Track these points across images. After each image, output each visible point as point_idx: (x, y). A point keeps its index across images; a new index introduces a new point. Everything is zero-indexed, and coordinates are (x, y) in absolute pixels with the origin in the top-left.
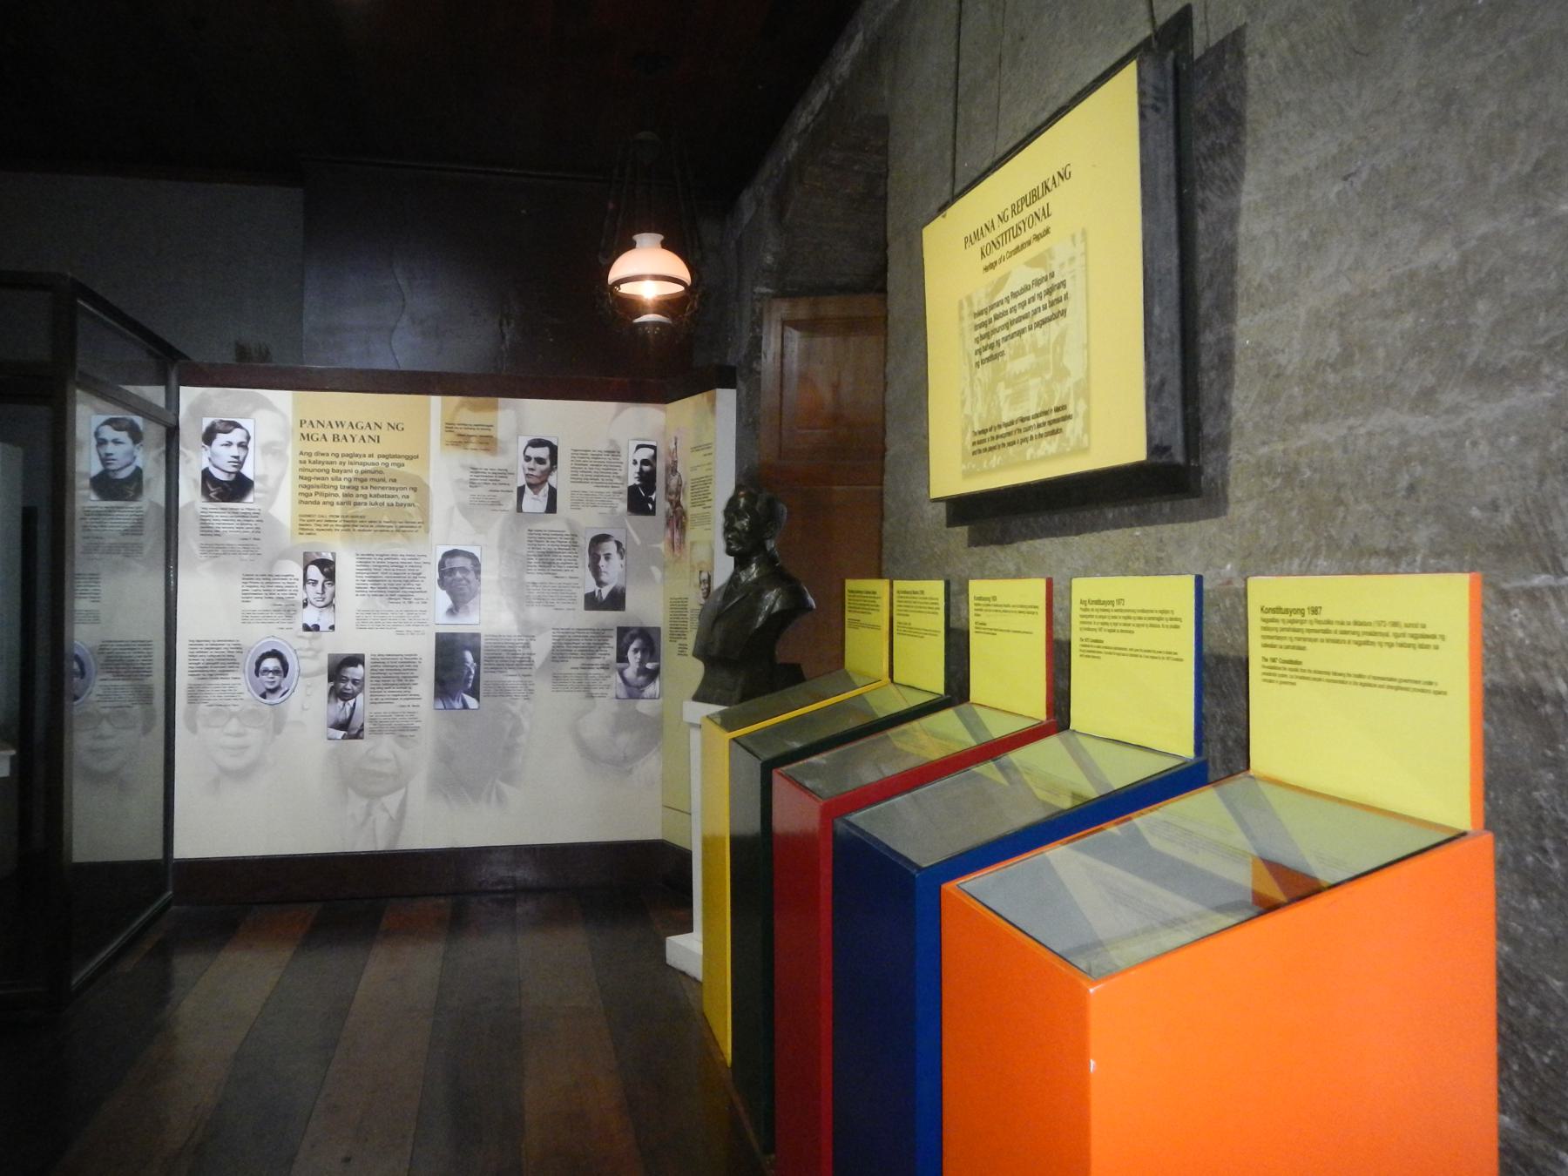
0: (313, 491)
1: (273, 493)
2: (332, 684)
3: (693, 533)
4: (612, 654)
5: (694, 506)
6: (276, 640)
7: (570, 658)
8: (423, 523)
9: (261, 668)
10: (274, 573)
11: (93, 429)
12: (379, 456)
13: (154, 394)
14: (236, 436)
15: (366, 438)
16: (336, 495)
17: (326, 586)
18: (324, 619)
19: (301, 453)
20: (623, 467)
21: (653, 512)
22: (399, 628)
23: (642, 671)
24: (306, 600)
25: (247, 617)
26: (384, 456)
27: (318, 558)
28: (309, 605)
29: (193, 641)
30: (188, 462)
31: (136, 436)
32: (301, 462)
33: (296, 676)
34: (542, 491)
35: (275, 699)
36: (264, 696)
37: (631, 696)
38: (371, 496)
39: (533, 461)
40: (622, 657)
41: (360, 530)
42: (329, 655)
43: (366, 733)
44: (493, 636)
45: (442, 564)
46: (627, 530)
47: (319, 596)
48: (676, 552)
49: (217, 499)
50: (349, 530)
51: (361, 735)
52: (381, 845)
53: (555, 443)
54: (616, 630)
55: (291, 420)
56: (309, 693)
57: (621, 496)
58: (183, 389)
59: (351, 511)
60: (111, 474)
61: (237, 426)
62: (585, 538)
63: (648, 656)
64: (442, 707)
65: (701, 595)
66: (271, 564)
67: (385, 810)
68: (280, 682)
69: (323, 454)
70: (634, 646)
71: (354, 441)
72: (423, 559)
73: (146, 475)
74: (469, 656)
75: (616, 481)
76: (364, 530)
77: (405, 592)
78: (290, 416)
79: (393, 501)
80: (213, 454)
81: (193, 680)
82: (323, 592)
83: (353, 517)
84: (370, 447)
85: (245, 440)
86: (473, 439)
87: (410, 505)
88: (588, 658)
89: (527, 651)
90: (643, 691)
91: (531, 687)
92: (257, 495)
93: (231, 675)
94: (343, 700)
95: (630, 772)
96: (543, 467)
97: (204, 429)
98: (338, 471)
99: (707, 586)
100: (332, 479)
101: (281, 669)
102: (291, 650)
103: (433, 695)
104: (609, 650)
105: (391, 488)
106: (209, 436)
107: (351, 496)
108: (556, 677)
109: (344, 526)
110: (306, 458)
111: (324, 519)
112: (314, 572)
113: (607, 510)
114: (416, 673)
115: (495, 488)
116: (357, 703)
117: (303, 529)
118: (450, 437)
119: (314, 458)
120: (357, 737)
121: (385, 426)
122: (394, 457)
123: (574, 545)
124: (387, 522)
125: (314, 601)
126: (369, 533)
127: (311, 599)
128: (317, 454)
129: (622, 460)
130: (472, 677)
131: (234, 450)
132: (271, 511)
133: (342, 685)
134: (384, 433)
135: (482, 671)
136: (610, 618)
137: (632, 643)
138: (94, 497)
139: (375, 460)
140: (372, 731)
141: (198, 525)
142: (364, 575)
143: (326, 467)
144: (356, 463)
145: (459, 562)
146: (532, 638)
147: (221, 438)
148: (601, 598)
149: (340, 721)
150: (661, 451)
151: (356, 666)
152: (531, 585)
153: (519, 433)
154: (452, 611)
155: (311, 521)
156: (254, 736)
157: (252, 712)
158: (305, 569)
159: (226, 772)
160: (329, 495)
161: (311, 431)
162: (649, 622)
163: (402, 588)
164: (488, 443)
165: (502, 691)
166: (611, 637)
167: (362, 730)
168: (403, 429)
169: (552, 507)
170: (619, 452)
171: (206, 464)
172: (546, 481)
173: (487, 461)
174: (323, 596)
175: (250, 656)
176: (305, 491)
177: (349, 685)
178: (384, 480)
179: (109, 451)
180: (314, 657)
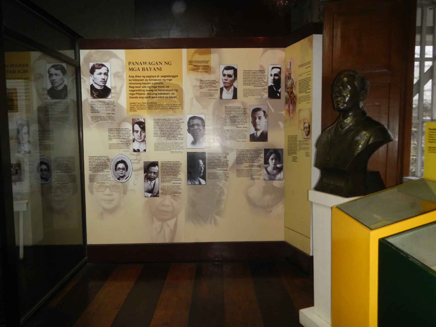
0: (135, 92)
1: (118, 94)
2: (146, 174)
3: (300, 106)
4: (262, 161)
5: (300, 92)
6: (123, 156)
7: (244, 162)
8: (180, 105)
9: (117, 168)
10: (121, 128)
11: (47, 70)
12: (162, 76)
13: (70, 53)
14: (103, 70)
15: (156, 69)
16: (144, 94)
17: (142, 133)
18: (142, 147)
19: (130, 76)
20: (266, 77)
21: (279, 98)
22: (172, 150)
23: (275, 168)
24: (134, 139)
25: (111, 147)
26: (163, 76)
27: (138, 121)
28: (135, 141)
29: (90, 157)
30: (85, 82)
31: (64, 72)
32: (129, 80)
33: (131, 171)
34: (231, 89)
35: (123, 180)
36: (119, 179)
37: (271, 179)
38: (159, 94)
39: (226, 76)
40: (266, 162)
41: (155, 109)
42: (144, 162)
43: (160, 195)
44: (211, 153)
45: (189, 123)
46: (268, 105)
47: (139, 137)
48: (291, 115)
49: (97, 97)
50: (150, 109)
51: (158, 195)
52: (167, 240)
53: (236, 68)
54: (263, 150)
55: (125, 63)
56: (137, 178)
57: (265, 91)
58: (81, 51)
59: (151, 100)
60: (55, 88)
61: (103, 65)
62: (250, 110)
63: (278, 162)
64: (191, 184)
65: (304, 134)
66: (119, 124)
67: (169, 226)
68: (125, 173)
69: (138, 77)
70: (271, 157)
71: (151, 70)
72: (181, 121)
73: (69, 88)
74: (201, 162)
75: (263, 84)
76: (156, 109)
77: (174, 135)
78: (124, 60)
79: (168, 96)
80: (94, 78)
81: (91, 173)
82: (141, 136)
83: (151, 103)
84: (158, 73)
85: (107, 72)
86: (201, 67)
87: (175, 97)
88: (251, 162)
89: (225, 159)
90: (276, 177)
91: (227, 175)
92: (113, 95)
93: (106, 170)
94: (150, 180)
95: (270, 212)
96: (231, 79)
97: (90, 68)
98: (145, 84)
99: (308, 130)
100: (143, 87)
101: (125, 168)
102: (129, 160)
103: (186, 179)
104: (261, 159)
105: (167, 90)
106: (92, 71)
107: (150, 94)
108: (238, 171)
109: (148, 107)
110: (132, 78)
111: (140, 104)
112: (137, 127)
113: (259, 97)
114: (179, 169)
115: (210, 88)
116: (156, 182)
117: (132, 109)
118: (191, 67)
119: (135, 78)
120: (156, 196)
121: (163, 63)
122: (168, 76)
123: (245, 113)
124: (166, 105)
125: (137, 139)
126: (159, 110)
127: (136, 138)
128: (136, 76)
129: (265, 74)
130: (202, 171)
131: (103, 76)
132: (118, 102)
133: (150, 174)
134: (163, 66)
135: (207, 168)
136: (261, 145)
137: (270, 156)
138: (49, 98)
139: (160, 78)
140: (162, 194)
141: (89, 108)
142: (157, 128)
143: (140, 82)
144: (152, 80)
145: (196, 121)
146: (228, 154)
147: (97, 71)
148: (257, 136)
149: (149, 189)
150: (283, 69)
151: (155, 166)
152: (227, 131)
153: (220, 64)
154: (194, 143)
155: (135, 105)
156: (116, 195)
157: (115, 186)
158: (133, 126)
159: (105, 210)
160: (141, 94)
161: (133, 66)
162: (278, 147)
163: (173, 133)
164: (207, 69)
165: (215, 177)
166: (262, 153)
167: (158, 193)
168: (171, 64)
169: (235, 97)
170: (264, 71)
171: (92, 82)
172: (232, 85)
173: (207, 77)
174: (141, 137)
175: (113, 162)
176: (132, 92)
177: (153, 175)
178: (164, 87)
179: (54, 79)
180: (138, 163)
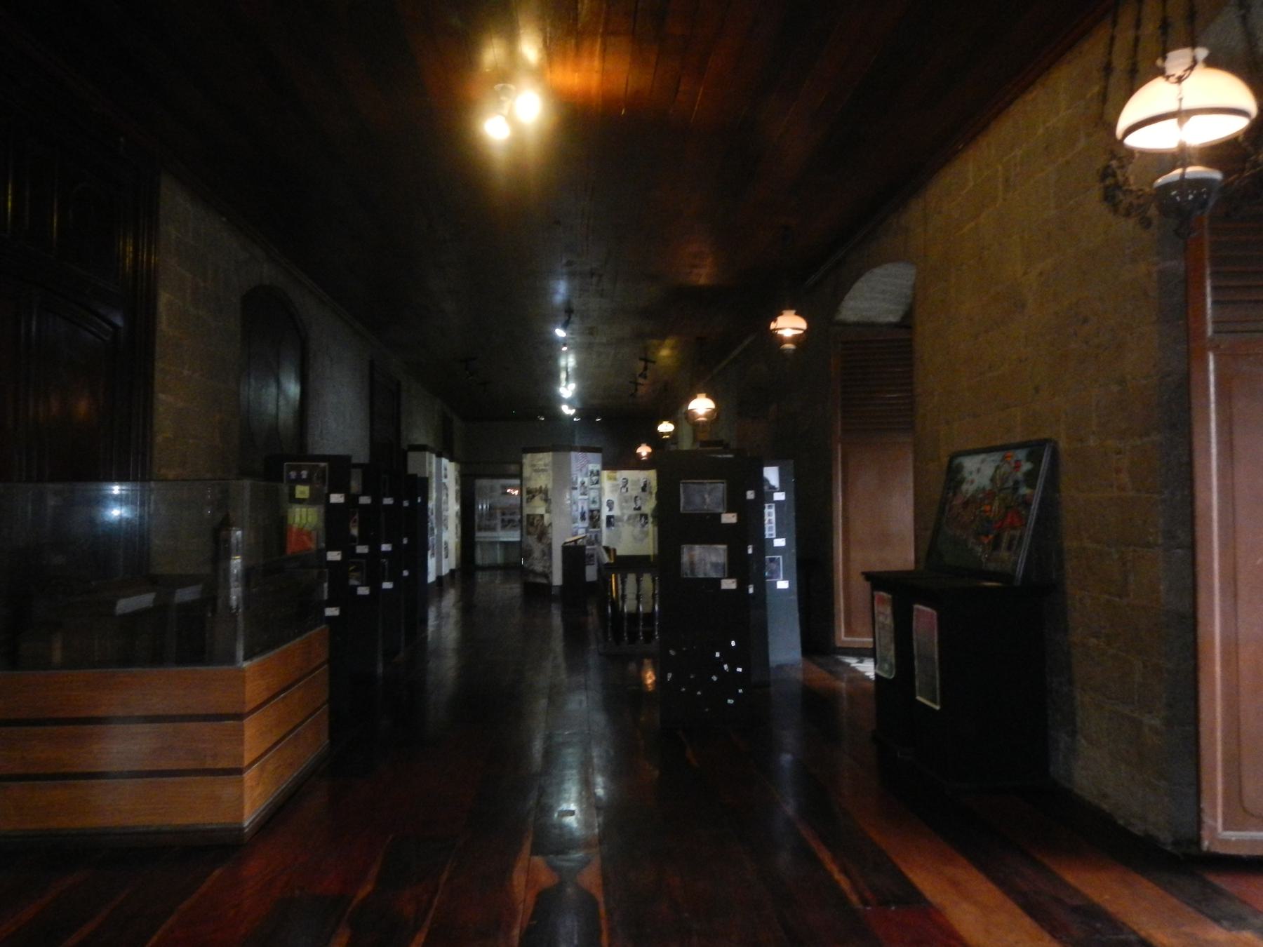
4: (639, 519)
40: (641, 519)
164: (615, 479)
165: (618, 526)
169: (627, 491)
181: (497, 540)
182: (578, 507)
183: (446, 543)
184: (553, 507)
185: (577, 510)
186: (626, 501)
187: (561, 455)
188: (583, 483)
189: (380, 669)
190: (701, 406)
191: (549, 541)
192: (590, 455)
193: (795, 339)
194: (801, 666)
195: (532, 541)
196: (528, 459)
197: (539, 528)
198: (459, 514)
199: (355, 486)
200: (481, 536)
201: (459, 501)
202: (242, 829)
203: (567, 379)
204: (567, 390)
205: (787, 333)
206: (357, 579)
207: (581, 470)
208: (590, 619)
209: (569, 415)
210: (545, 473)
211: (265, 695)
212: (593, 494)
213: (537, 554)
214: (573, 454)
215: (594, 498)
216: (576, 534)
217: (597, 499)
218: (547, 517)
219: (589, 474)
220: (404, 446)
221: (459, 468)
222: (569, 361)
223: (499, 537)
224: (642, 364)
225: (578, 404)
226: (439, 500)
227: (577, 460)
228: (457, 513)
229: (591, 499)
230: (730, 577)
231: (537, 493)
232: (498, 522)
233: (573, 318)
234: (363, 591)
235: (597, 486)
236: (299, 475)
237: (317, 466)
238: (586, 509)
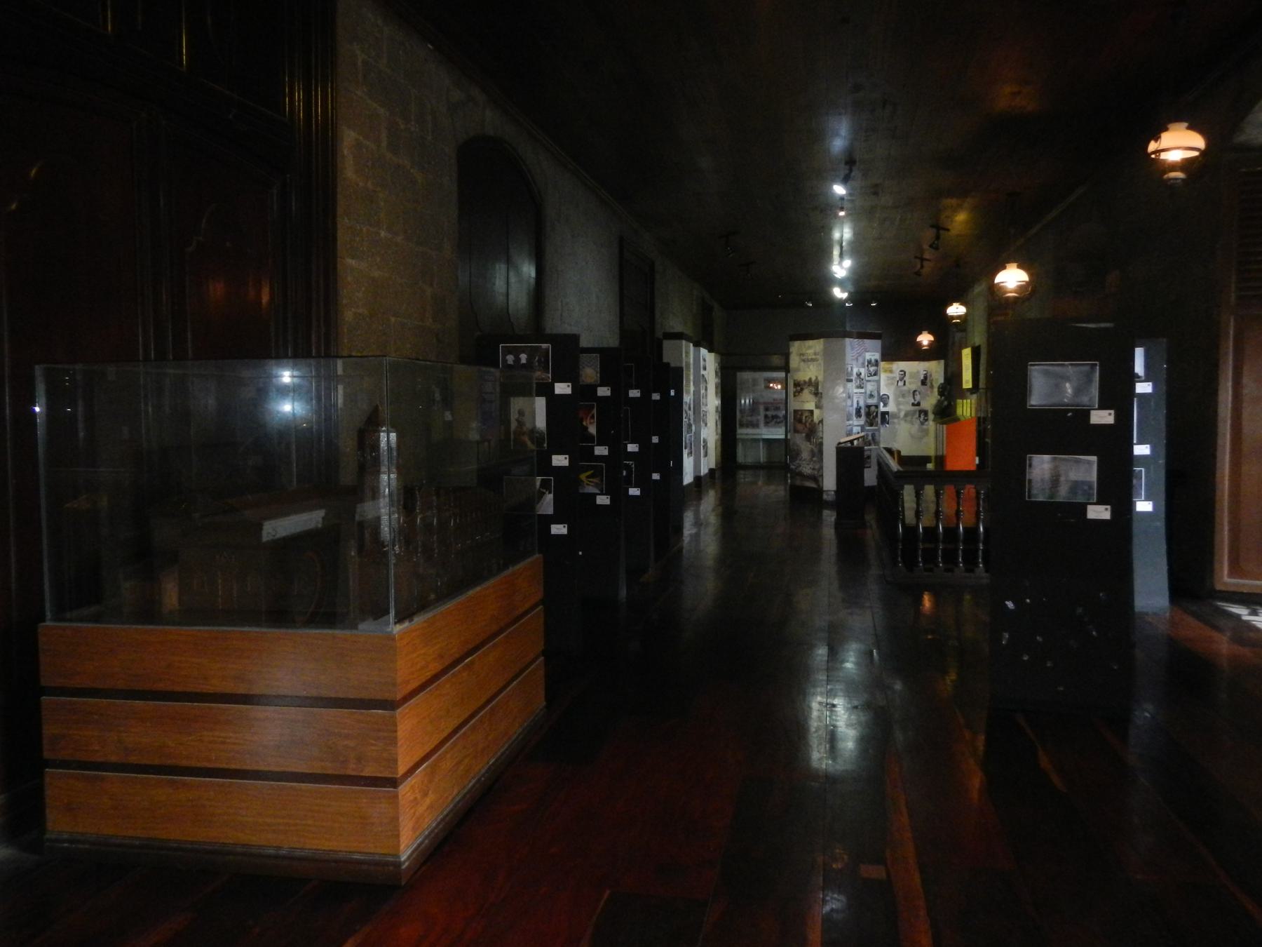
4: (917, 416)
40: (920, 416)
108: (906, 421)
164: (891, 371)
165: (894, 423)
169: (904, 384)
181: (759, 437)
182: (852, 402)
183: (705, 441)
184: (824, 402)
185: (852, 406)
186: (903, 396)
187: (835, 342)
188: (859, 375)
189: (623, 593)
190: (1012, 278)
191: (820, 440)
192: (868, 342)
193: (1186, 165)
194: (1168, 614)
195: (799, 440)
196: (796, 347)
197: (808, 424)
198: (720, 409)
199: (590, 373)
200: (742, 432)
201: (720, 395)
202: (398, 865)
203: (841, 255)
204: (841, 268)
205: (1174, 156)
206: (596, 485)
207: (857, 359)
208: (869, 531)
209: (841, 299)
210: (815, 363)
211: (435, 667)
212: (870, 387)
213: (805, 455)
214: (848, 340)
215: (871, 392)
216: (849, 434)
217: (875, 393)
218: (817, 412)
219: (866, 364)
220: (659, 334)
221: (719, 360)
222: (843, 233)
223: (761, 434)
224: (934, 230)
225: (851, 288)
226: (697, 393)
227: (853, 349)
228: (717, 408)
229: (868, 392)
230: (1099, 503)
231: (804, 387)
232: (761, 418)
233: (856, 173)
234: (603, 500)
235: (875, 378)
236: (517, 359)
237: (541, 346)
238: (862, 404)
